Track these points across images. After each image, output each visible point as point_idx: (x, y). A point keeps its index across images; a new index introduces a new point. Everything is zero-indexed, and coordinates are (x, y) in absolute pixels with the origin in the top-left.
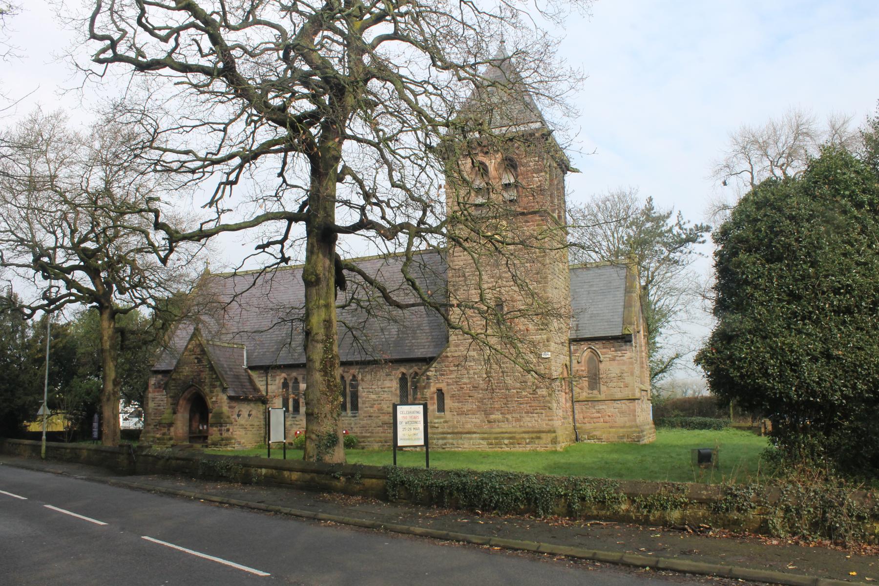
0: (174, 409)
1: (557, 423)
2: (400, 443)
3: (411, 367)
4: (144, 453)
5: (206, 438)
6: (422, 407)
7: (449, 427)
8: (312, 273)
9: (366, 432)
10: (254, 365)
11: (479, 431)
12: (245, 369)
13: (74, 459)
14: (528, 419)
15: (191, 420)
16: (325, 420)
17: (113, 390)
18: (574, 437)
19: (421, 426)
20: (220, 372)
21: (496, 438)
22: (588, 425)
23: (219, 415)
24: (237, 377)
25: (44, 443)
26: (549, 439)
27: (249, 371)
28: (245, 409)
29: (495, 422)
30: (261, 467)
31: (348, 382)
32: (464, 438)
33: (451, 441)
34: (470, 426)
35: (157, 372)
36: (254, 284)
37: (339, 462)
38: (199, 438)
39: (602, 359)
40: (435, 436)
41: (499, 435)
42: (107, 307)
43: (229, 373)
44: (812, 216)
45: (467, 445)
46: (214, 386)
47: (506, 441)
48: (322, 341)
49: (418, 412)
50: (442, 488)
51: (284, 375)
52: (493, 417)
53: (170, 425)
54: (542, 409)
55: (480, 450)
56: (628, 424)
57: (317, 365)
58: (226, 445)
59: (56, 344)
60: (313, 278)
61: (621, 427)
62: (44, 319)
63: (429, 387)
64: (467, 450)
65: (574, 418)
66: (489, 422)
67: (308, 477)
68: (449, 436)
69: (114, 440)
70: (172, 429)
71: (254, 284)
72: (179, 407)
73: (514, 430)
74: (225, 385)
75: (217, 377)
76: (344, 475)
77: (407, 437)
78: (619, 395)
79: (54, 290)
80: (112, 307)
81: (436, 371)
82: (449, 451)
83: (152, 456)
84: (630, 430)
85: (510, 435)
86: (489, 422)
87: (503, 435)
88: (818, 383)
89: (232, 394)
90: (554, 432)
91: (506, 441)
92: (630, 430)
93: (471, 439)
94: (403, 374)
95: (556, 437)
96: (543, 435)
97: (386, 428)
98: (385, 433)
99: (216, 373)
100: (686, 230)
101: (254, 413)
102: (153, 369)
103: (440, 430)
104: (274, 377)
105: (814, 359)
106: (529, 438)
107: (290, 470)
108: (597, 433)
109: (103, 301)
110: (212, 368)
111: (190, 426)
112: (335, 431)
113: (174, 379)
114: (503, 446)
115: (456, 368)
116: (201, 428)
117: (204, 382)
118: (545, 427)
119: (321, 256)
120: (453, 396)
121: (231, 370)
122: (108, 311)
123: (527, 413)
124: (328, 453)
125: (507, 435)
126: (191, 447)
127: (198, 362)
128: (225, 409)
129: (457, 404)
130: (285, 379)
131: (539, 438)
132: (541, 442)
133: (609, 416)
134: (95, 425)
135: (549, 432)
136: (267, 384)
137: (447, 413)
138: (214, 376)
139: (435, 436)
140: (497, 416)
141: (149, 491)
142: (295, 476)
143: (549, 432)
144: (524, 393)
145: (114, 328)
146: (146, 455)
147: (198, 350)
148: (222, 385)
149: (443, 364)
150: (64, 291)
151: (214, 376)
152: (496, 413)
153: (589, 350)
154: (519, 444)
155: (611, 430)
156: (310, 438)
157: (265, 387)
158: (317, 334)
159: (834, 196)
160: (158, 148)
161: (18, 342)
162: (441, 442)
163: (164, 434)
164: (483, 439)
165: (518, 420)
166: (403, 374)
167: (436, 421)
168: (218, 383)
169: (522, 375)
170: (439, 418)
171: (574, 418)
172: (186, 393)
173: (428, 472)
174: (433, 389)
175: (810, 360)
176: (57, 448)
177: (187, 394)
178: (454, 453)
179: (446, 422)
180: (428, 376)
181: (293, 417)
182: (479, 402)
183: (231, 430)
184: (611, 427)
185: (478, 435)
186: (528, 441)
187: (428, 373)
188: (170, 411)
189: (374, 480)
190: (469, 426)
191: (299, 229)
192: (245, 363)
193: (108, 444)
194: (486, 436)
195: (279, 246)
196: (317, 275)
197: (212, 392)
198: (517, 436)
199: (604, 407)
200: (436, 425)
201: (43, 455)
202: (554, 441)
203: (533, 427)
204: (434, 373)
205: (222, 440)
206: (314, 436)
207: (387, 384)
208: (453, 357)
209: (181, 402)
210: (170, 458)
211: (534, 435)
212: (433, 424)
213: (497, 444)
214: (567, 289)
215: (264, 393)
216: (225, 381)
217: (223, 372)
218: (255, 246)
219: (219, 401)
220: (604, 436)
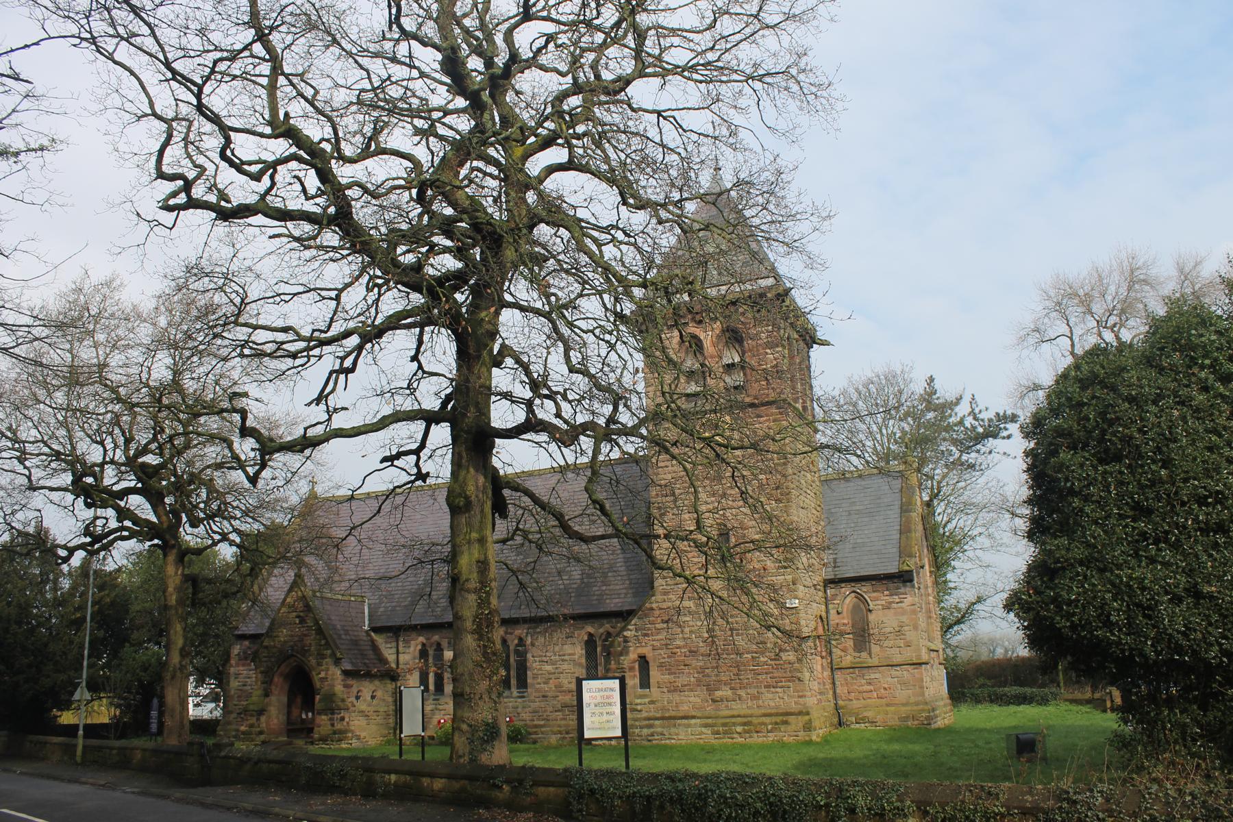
0: (265, 690)
1: (811, 701)
2: (587, 735)
3: (601, 626)
4: (223, 754)
5: (311, 730)
6: (617, 681)
7: (657, 710)
8: (460, 495)
9: (538, 720)
10: (379, 625)
12: (367, 632)
13: (123, 763)
14: (770, 696)
15: (290, 705)
16: (481, 703)
17: (180, 662)
18: (836, 720)
19: (617, 709)
20: (331, 636)
21: (724, 725)
22: (855, 702)
23: (330, 697)
24: (355, 643)
25: (80, 742)
26: (801, 725)
27: (373, 634)
28: (367, 688)
29: (722, 700)
30: (389, 773)
31: (512, 648)
33: (659, 730)
35: (243, 637)
36: (379, 511)
37: (501, 762)
38: (301, 730)
39: (871, 607)
40: (637, 723)
41: (728, 720)
42: (173, 546)
43: (343, 637)
44: (1160, 397)
45: (684, 735)
46: (323, 657)
47: (739, 729)
48: (476, 591)
49: (612, 690)
50: (649, 798)
51: (421, 639)
52: (718, 694)
53: (261, 712)
54: (789, 681)
55: (701, 741)
56: (912, 700)
57: (469, 625)
58: (340, 740)
59: (102, 598)
60: (462, 502)
61: (903, 705)
62: (86, 564)
63: (627, 653)
64: (683, 742)
65: (835, 692)
67: (456, 785)
68: (657, 722)
69: (180, 736)
70: (263, 719)
71: (379, 511)
72: (273, 687)
73: (749, 712)
74: (338, 655)
75: (327, 643)
76: (508, 782)
77: (597, 725)
78: (898, 659)
79: (99, 522)
80: (180, 546)
81: (637, 630)
82: (658, 745)
83: (235, 758)
84: (915, 708)
87: (733, 720)
88: (1184, 634)
89: (349, 667)
90: (808, 713)
91: (739, 729)
92: (915, 708)
93: (689, 726)
94: (590, 635)
95: (810, 720)
96: (791, 719)
97: (567, 713)
98: (565, 719)
99: (325, 638)
100: (983, 420)
101: (379, 694)
102: (236, 633)
103: (644, 714)
104: (407, 642)
105: (1177, 600)
106: (771, 724)
107: (432, 776)
108: (870, 714)
109: (168, 537)
110: (320, 631)
111: (289, 713)
112: (495, 719)
113: (266, 647)
114: (735, 736)
115: (665, 625)
116: (304, 716)
117: (309, 650)
118: (794, 707)
119: (472, 470)
120: (661, 666)
121: (347, 632)
122: (175, 551)
123: (767, 687)
124: (485, 750)
125: (739, 720)
126: (290, 743)
127: (300, 623)
128: (339, 688)
130: (424, 645)
131: (786, 723)
132: (788, 728)
133: (885, 689)
134: (154, 713)
135: (800, 713)
136: (398, 653)
137: (654, 689)
138: (323, 642)
139: (637, 723)
140: (724, 693)
141: (229, 809)
142: (438, 784)
143: (800, 713)
144: (762, 659)
145: (183, 574)
146: (226, 757)
147: (300, 605)
148: (334, 654)
149: (646, 620)
150: (113, 524)
151: (323, 642)
152: (724, 687)
153: (853, 595)
154: (757, 732)
155: (888, 708)
156: (459, 729)
157: (394, 657)
158: (467, 580)
159: (1190, 367)
160: (246, 325)
161: (48, 596)
162: (645, 731)
163: (251, 726)
164: (706, 726)
165: (754, 698)
166: (590, 635)
167: (638, 701)
168: (329, 652)
169: (759, 633)
171: (835, 692)
172: (283, 667)
173: (628, 775)
174: (633, 656)
175: (1170, 601)
176: (100, 748)
177: (284, 668)
178: (665, 747)
179: (652, 702)
180: (625, 637)
181: (434, 700)
182: (698, 673)
183: (347, 720)
184: (887, 705)
185: (698, 721)
186: (770, 727)
187: (625, 633)
188: (259, 692)
189: (552, 789)
190: (685, 708)
191: (441, 434)
192: (367, 623)
193: (172, 741)
194: (710, 721)
195: (414, 457)
196: (467, 498)
197: (319, 664)
198: (755, 720)
199: (877, 676)
200: (639, 707)
201: (78, 759)
202: (808, 727)
203: (777, 707)
204: (633, 632)
205: (335, 733)
206: (464, 727)
207: (568, 649)
208: (661, 609)
209: (276, 679)
210: (259, 761)
211: (779, 719)
213: (725, 733)
214: (819, 509)
215: (394, 666)
216: (338, 648)
217: (335, 636)
218: (380, 458)
219: (331, 677)
220: (879, 718)
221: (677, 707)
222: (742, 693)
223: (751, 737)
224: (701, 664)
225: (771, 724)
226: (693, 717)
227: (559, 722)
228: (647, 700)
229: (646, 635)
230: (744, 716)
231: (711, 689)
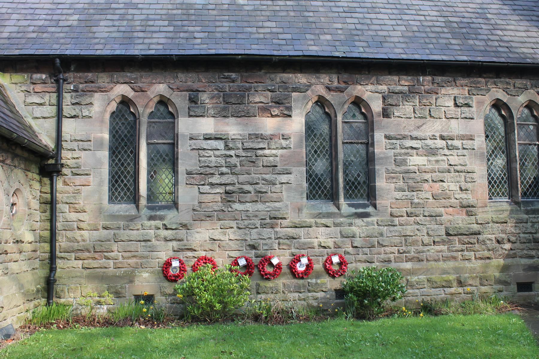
94: (498, 105)
97: (458, 246)
136: (59, 116)
181: (151, 218)
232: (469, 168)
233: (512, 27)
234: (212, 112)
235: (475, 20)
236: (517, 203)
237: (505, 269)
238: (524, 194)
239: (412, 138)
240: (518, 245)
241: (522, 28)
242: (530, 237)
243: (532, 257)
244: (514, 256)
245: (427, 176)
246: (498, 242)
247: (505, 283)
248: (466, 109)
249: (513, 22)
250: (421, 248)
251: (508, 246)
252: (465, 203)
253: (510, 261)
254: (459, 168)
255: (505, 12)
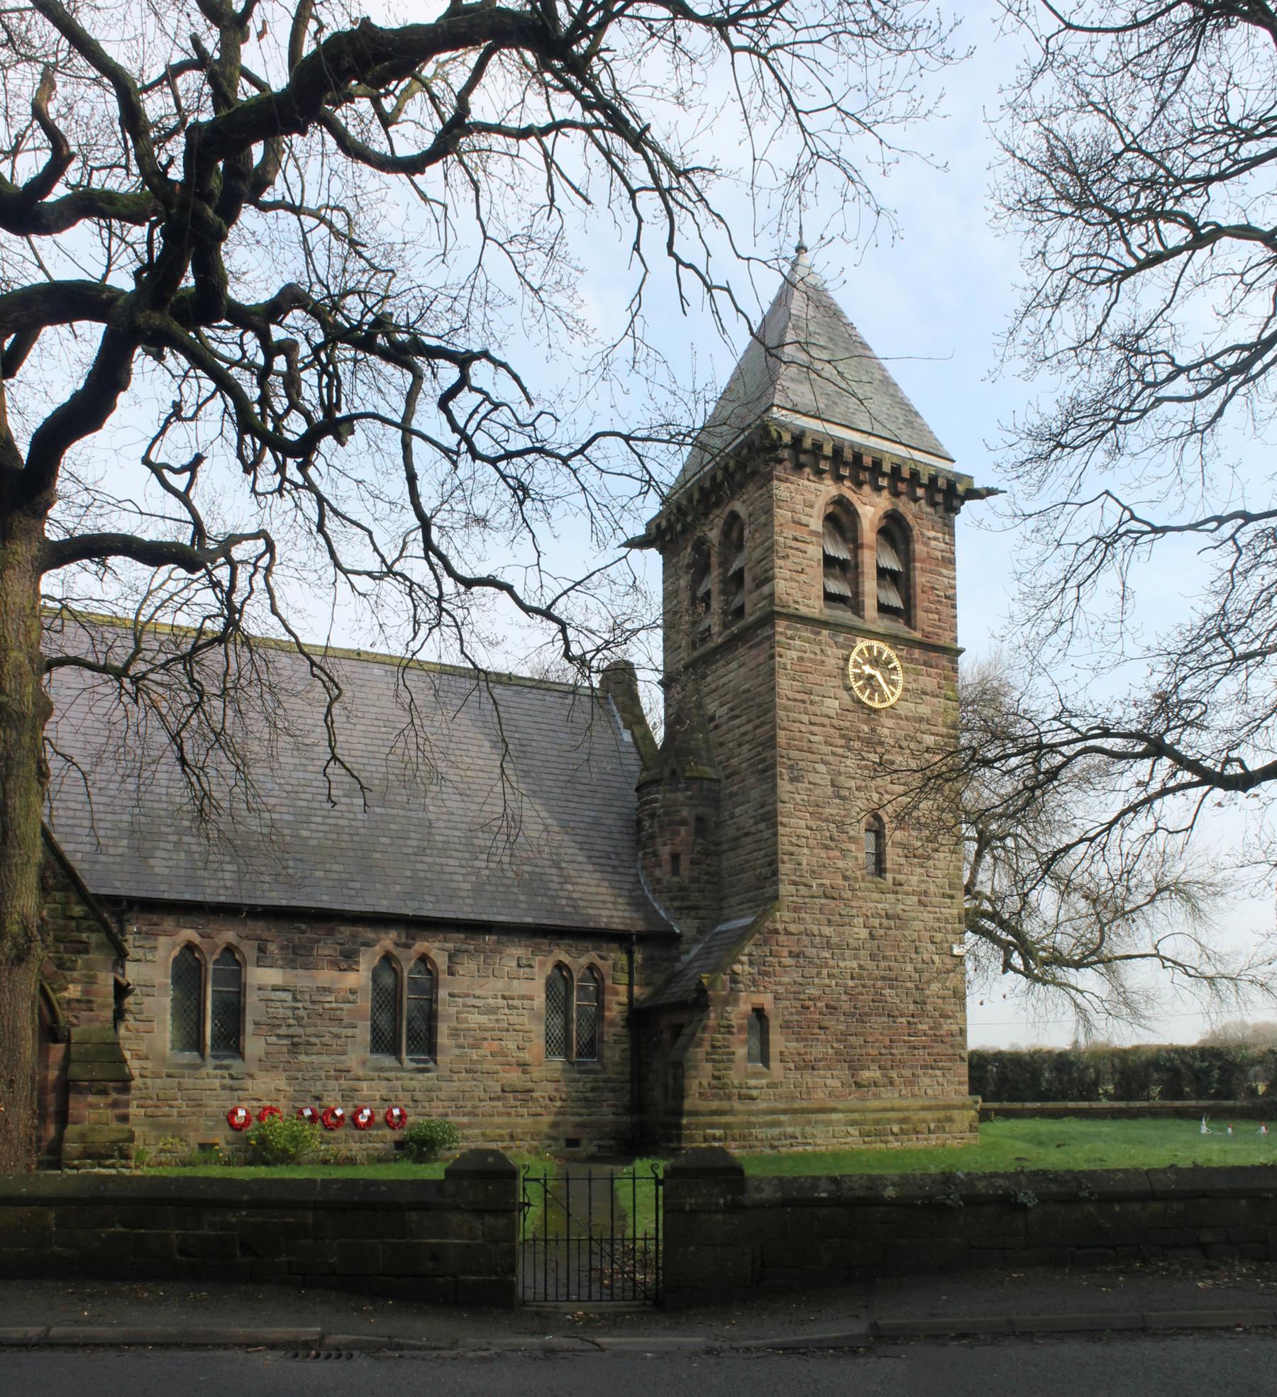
9: (454, 1114)
11: (840, 1106)
21: (877, 1122)
32: (816, 1122)
33: (789, 1130)
34: (821, 1095)
41: (880, 1115)
51: (189, 934)
52: (866, 1074)
54: (950, 1060)
55: (847, 1147)
63: (736, 1001)
64: (823, 1148)
66: (858, 1085)
68: (783, 1118)
73: (904, 1103)
85: (901, 1115)
86: (858, 1085)
93: (829, 1123)
94: (560, 966)
96: (955, 1114)
97: (512, 1102)
103: (763, 1105)
106: (933, 1121)
114: (891, 1138)
120: (786, 1026)
123: (924, 1067)
129: (795, 1044)
131: (950, 1119)
137: (775, 1064)
152: (874, 1067)
164: (853, 1123)
165: (909, 1082)
166: (560, 966)
167: (753, 1082)
169: (917, 988)
170: (756, 1075)
174: (745, 1007)
180: (735, 973)
181: (217, 1067)
182: (839, 1041)
185: (841, 1115)
194: (856, 1116)
198: (916, 1116)
200: (755, 1093)
207: (519, 987)
208: (788, 933)
211: (941, 1114)
212: (744, 1091)
221: (808, 1093)
222: (894, 1074)
223: (909, 1140)
224: (842, 1027)
225: (933, 1121)
226: (834, 1110)
227: (496, 1120)
228: (764, 1081)
229: (767, 974)
230: (900, 1110)
231: (854, 1067)
232: (527, 1027)
233: (584, 880)
234: (280, 963)
235: (548, 871)
236: (572, 1063)
237: (554, 1125)
238: (580, 1054)
239: (475, 997)
240: (569, 1103)
241: (593, 882)
242: (581, 1095)
243: (581, 1115)
244: (564, 1114)
245: (487, 1035)
246: (551, 1100)
247: (555, 1139)
248: (527, 970)
249: (586, 874)
250: (477, 1103)
251: (558, 1104)
252: (521, 1061)
253: (559, 1118)
254: (518, 1027)
255: (581, 859)
